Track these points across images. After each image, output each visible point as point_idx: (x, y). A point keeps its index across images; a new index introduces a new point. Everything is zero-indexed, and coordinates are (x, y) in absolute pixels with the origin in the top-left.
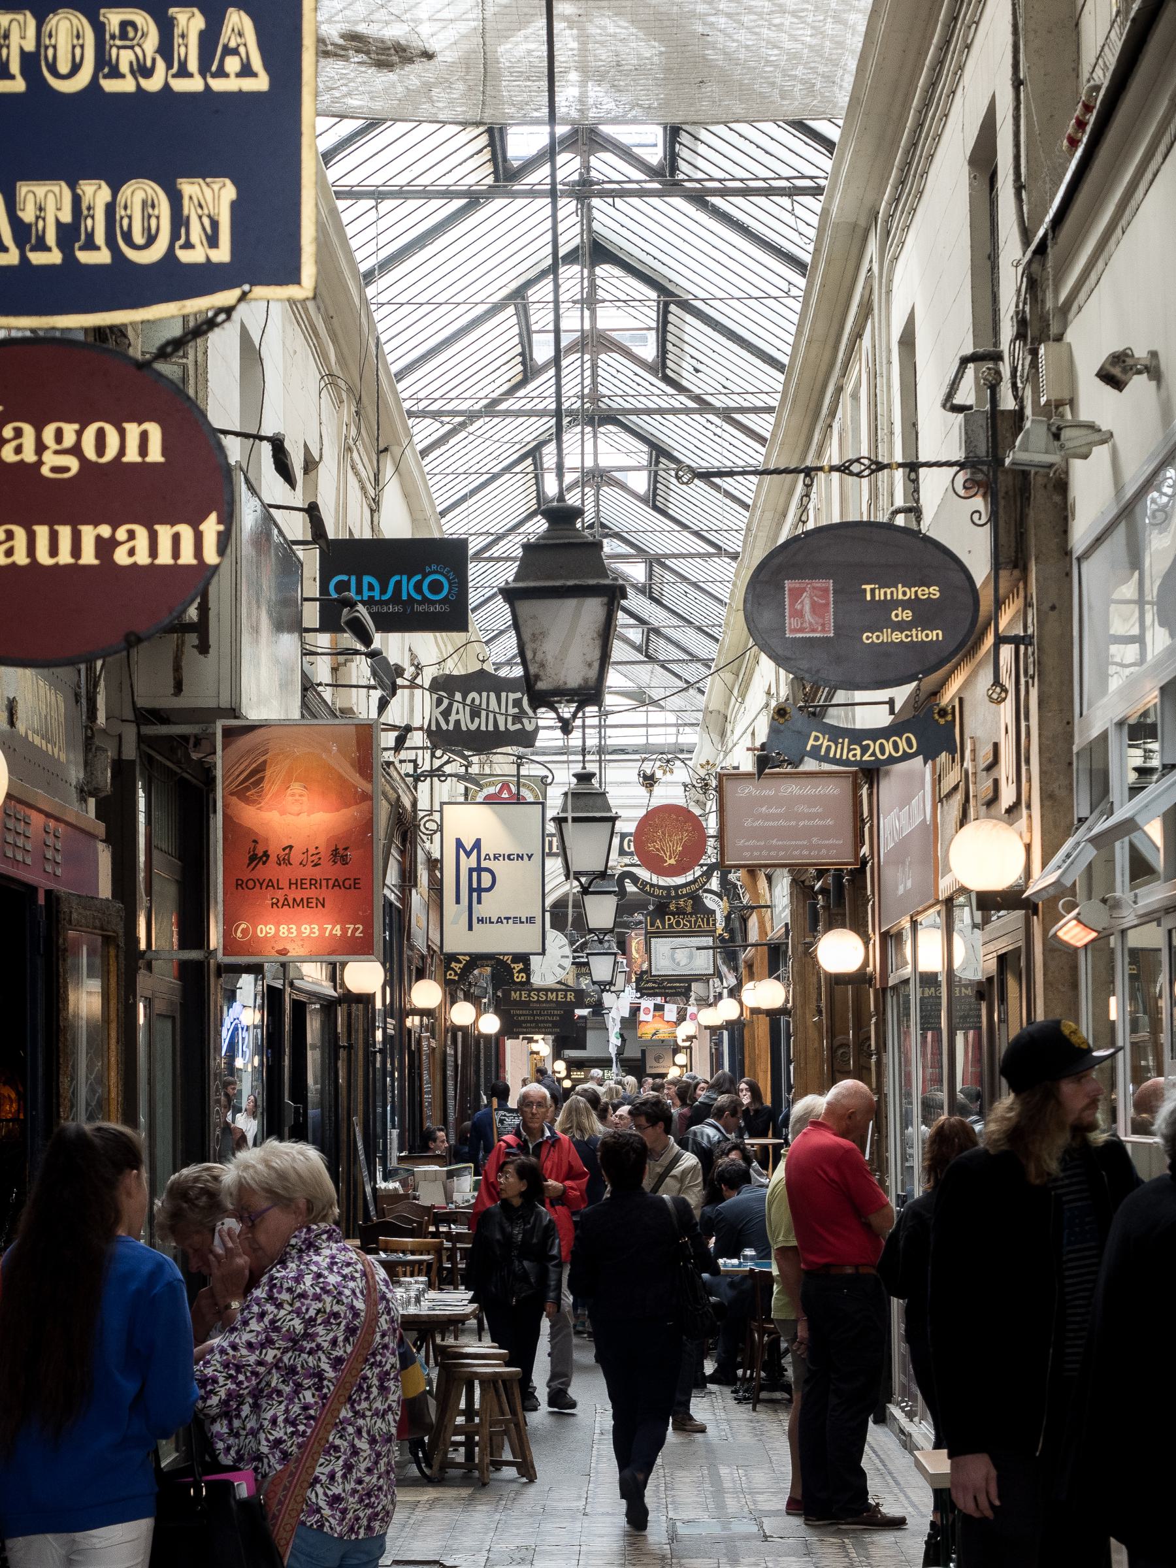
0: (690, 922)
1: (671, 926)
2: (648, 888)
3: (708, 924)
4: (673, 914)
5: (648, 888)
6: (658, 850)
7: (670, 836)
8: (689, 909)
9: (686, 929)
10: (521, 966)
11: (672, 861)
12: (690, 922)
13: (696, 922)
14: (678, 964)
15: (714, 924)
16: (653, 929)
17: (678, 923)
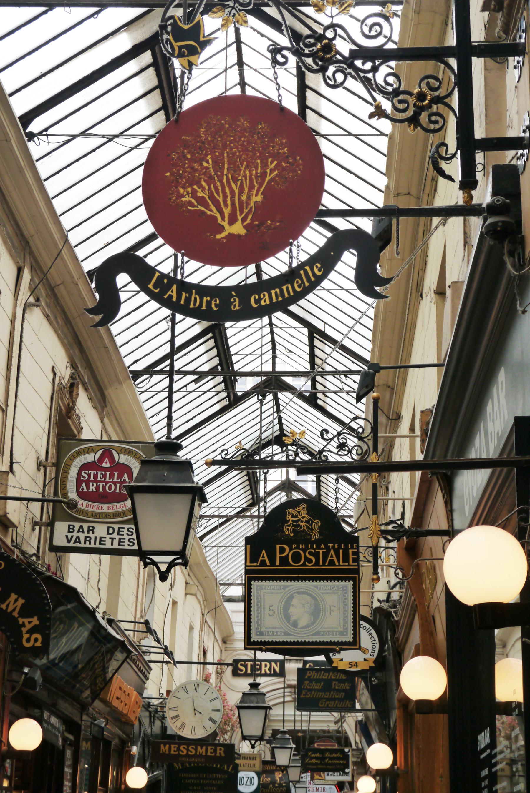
0: (316, 555)
1: (284, 561)
2: (173, 291)
3: (346, 560)
4: (289, 542)
5: (173, 291)
6: (202, 201)
7: (234, 168)
8: (315, 535)
9: (310, 566)
10: (35, 621)
11: (238, 229)
12: (316, 555)
13: (326, 555)
14: (295, 624)
15: (356, 560)
16: (255, 566)
17: (296, 558)
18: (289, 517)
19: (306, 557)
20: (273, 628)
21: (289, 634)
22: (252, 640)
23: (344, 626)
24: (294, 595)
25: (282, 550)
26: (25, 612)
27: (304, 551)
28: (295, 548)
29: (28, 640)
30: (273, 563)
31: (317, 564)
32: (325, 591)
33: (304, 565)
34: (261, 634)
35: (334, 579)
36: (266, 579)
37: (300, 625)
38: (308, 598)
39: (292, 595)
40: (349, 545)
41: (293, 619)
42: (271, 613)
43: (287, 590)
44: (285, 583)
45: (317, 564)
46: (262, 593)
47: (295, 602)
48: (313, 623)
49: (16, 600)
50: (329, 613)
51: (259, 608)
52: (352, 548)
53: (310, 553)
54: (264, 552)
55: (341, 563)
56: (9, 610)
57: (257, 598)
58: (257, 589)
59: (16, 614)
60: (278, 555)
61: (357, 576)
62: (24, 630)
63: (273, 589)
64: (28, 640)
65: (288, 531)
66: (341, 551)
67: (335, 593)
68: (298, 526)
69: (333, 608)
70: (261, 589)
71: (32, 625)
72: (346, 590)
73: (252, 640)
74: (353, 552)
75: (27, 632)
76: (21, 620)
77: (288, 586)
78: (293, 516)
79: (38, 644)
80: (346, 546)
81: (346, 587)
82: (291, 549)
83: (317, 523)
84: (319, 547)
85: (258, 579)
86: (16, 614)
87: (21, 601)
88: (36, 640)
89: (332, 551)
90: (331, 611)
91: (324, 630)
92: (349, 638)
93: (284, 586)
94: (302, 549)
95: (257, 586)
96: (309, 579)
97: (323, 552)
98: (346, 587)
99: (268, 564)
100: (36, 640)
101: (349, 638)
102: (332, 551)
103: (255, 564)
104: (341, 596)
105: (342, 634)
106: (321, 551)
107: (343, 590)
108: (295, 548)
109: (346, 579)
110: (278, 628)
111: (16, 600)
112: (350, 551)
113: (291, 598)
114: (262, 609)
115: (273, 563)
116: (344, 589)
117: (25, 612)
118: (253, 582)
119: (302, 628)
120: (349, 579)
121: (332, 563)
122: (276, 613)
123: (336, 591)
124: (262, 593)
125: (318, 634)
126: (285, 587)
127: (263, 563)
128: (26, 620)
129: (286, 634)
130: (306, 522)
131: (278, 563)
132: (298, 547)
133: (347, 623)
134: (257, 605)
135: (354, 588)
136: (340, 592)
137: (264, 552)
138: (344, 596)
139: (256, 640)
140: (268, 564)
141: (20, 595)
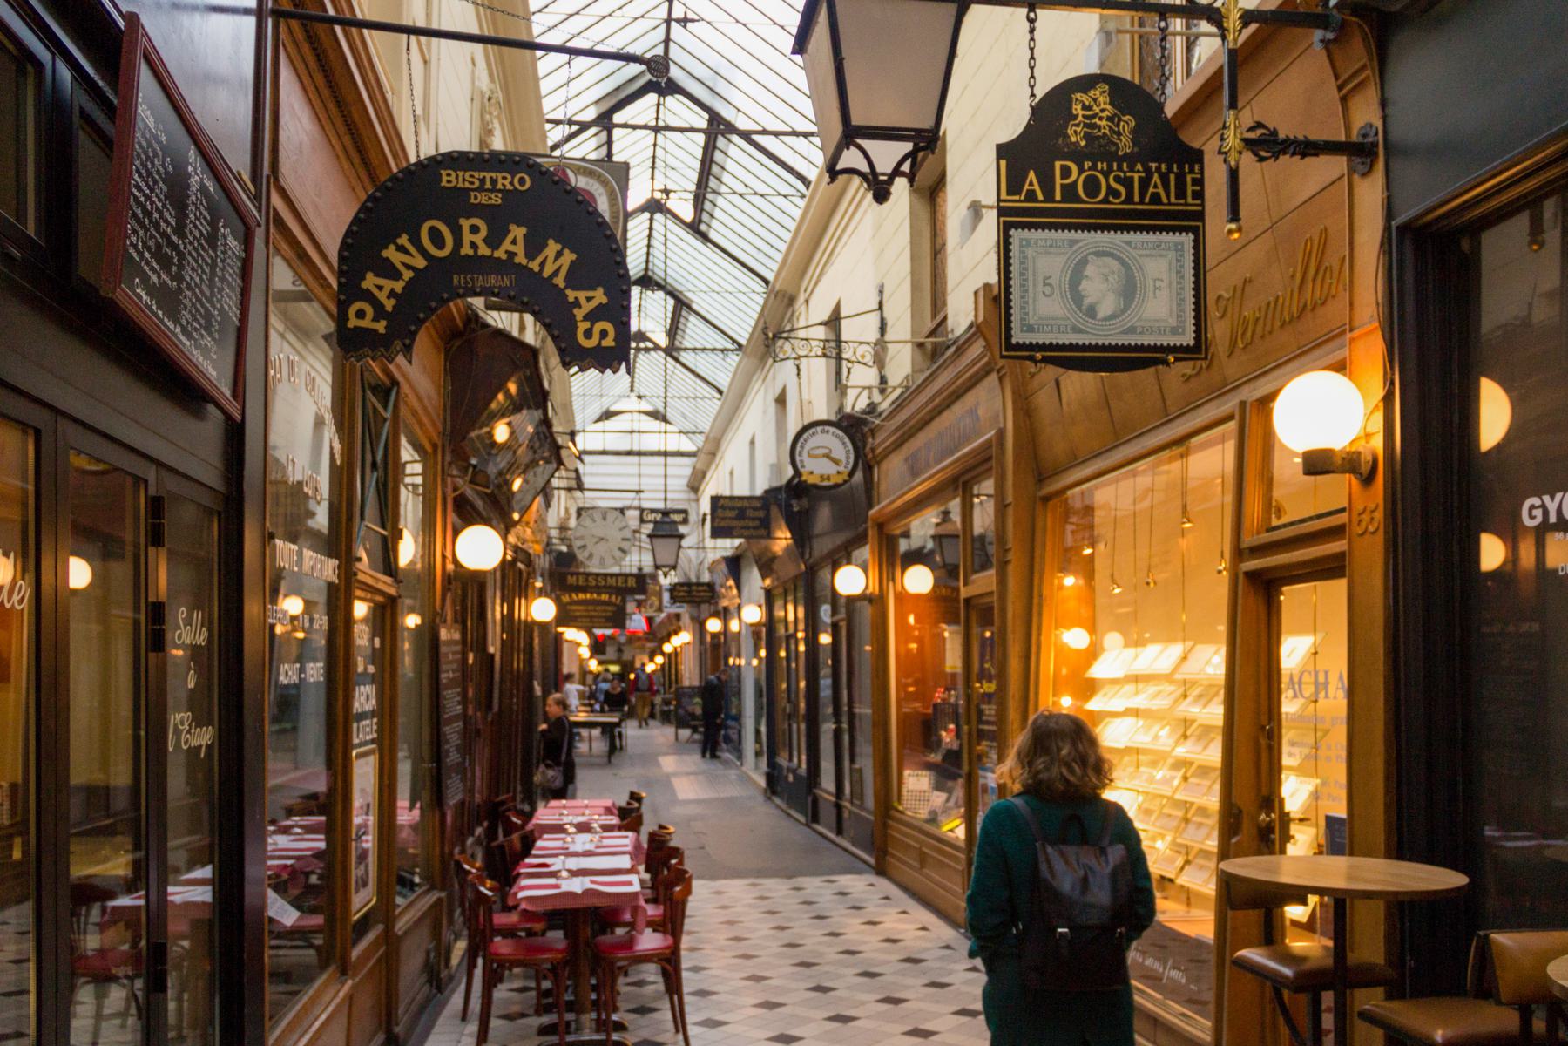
0: (1127, 182)
1: (1070, 192)
3: (1181, 193)
4: (1078, 156)
8: (1125, 144)
9: (1116, 204)
10: (600, 296)
12: (1127, 182)
13: (1144, 184)
14: (1091, 312)
15: (1199, 195)
16: (1018, 201)
17: (1092, 187)
18: (1077, 109)
19: (1110, 189)
20: (1052, 319)
21: (1081, 331)
22: (1014, 341)
23: (1178, 316)
24: (1089, 258)
25: (1066, 172)
26: (577, 278)
27: (1106, 174)
28: (1090, 169)
29: (588, 334)
30: (1049, 197)
31: (1129, 199)
32: (1144, 252)
33: (1105, 200)
34: (1031, 329)
35: (1161, 229)
36: (1036, 226)
37: (1101, 315)
38: (1114, 264)
39: (1086, 257)
40: (1187, 166)
41: (1087, 302)
42: (1048, 290)
43: (1075, 248)
44: (1073, 235)
45: (1129, 199)
46: (1030, 252)
47: (1090, 270)
48: (1123, 311)
49: (559, 254)
50: (1151, 295)
51: (1026, 280)
52: (1192, 171)
53: (1117, 179)
54: (1032, 174)
55: (1173, 200)
56: (546, 274)
57: (1022, 263)
58: (1021, 246)
59: (560, 281)
60: (1058, 181)
61: (1200, 224)
62: (579, 314)
63: (1051, 246)
64: (588, 334)
65: (1075, 134)
66: (1172, 177)
67: (1161, 256)
68: (1094, 126)
69: (1158, 283)
70: (1029, 244)
71: (593, 304)
72: (1182, 250)
73: (1014, 341)
74: (1193, 179)
75: (586, 318)
76: (571, 295)
77: (1077, 241)
78: (1085, 107)
79: (609, 342)
80: (1181, 167)
81: (1182, 244)
82: (1081, 171)
83: (1128, 123)
84: (1132, 169)
85: (1023, 226)
86: (560, 281)
87: (569, 257)
88: (604, 334)
89: (1156, 177)
90: (1156, 288)
91: (1143, 323)
92: (1188, 339)
93: (1071, 241)
94: (1102, 172)
95: (1021, 240)
96: (1116, 228)
97: (1140, 178)
98: (1182, 244)
99: (1041, 197)
100: (604, 334)
101: (1188, 339)
102: (1156, 177)
103: (1017, 198)
104: (1174, 261)
105: (1174, 331)
106: (1136, 176)
107: (1176, 250)
108: (1090, 169)
109: (1181, 229)
110: (1062, 319)
111: (559, 254)
112: (1189, 178)
113: (1084, 262)
114: (1030, 283)
115: (1049, 197)
116: (1179, 249)
117: (577, 278)
118: (1012, 232)
119: (1105, 319)
120: (1185, 229)
121: (1156, 199)
122: (1057, 291)
123: (1164, 253)
124: (1030, 252)
125: (1132, 330)
126: (1073, 242)
127: (1031, 196)
128: (582, 295)
129: (1076, 330)
130: (1109, 119)
131: (1058, 197)
132: (1094, 168)
133: (1183, 311)
134: (1022, 274)
135: (1196, 247)
136: (1172, 255)
137: (1032, 174)
138: (1178, 261)
139: (1021, 341)
140: (1041, 197)
141: (566, 243)
